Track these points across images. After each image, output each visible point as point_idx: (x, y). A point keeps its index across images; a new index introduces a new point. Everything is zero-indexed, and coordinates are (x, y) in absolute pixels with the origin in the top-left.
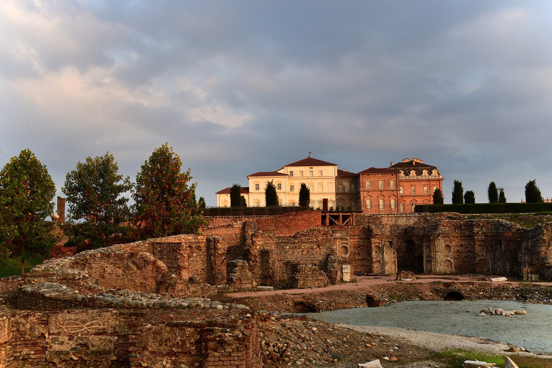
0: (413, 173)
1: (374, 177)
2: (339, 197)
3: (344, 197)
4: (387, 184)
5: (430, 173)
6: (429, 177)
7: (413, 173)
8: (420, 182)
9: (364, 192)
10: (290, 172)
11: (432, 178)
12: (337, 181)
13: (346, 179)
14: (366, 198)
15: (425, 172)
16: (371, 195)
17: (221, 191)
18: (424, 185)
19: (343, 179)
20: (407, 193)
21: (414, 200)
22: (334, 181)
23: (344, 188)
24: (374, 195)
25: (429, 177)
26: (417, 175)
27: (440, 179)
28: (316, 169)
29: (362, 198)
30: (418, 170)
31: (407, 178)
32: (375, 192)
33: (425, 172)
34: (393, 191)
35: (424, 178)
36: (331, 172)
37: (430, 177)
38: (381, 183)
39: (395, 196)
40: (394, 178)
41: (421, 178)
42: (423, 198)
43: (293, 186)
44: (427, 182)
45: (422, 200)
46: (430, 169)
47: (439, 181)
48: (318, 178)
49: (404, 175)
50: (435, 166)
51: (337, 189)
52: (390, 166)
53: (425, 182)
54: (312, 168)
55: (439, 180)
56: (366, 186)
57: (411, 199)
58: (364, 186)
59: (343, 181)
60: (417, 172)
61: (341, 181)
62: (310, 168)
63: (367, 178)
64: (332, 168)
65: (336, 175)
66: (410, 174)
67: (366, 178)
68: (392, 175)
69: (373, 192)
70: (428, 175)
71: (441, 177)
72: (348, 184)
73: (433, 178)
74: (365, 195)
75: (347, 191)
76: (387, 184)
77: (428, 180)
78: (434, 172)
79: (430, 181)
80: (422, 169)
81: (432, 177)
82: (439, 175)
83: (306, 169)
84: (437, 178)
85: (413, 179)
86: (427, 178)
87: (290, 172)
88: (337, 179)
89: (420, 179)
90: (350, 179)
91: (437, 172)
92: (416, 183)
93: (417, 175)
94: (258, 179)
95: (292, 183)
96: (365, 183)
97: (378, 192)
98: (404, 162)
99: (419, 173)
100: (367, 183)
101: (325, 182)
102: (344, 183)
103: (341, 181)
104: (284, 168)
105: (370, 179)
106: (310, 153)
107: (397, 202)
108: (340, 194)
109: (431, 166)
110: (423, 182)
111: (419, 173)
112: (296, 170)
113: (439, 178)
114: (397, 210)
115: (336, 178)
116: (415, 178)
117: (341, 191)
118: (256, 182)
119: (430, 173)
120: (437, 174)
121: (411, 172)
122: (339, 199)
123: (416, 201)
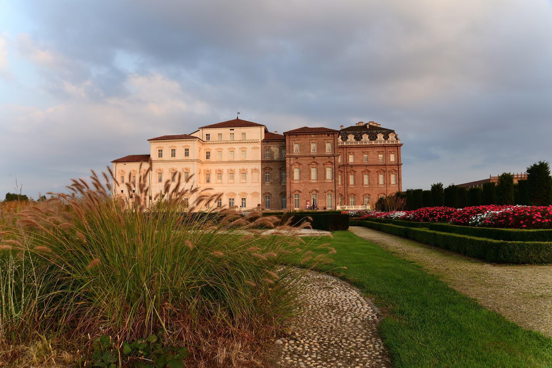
0: (365, 137)
1: (304, 139)
2: (266, 166)
3: (271, 166)
4: (321, 147)
5: (386, 137)
6: (385, 142)
7: (365, 137)
8: (373, 148)
9: (291, 158)
10: (207, 135)
11: (389, 144)
12: (263, 146)
13: (275, 143)
14: (293, 166)
15: (380, 137)
16: (300, 162)
17: (121, 159)
18: (379, 153)
19: (270, 143)
20: (358, 162)
21: (367, 170)
22: (260, 146)
23: (272, 154)
24: (305, 162)
25: (385, 142)
26: (370, 140)
27: (398, 144)
28: (238, 131)
29: (288, 166)
30: (372, 134)
31: (359, 143)
32: (305, 158)
33: (380, 137)
34: (329, 156)
35: (379, 143)
36: (257, 134)
37: (387, 143)
38: (313, 146)
39: (332, 163)
40: (331, 140)
41: (375, 144)
42: (377, 168)
43: (209, 153)
44: (382, 148)
45: (377, 170)
46: (387, 133)
47: (398, 146)
48: (240, 142)
49: (354, 140)
50: (393, 130)
51: (263, 155)
52: (341, 129)
53: (380, 148)
54: (233, 130)
55: (398, 146)
56: (293, 151)
57: (363, 170)
58: (291, 150)
59: (271, 145)
60: (370, 137)
61: (269, 146)
62: (231, 130)
63: (296, 139)
64: (258, 129)
65: (263, 138)
66: (362, 138)
67: (293, 139)
68: (328, 135)
69: (303, 158)
70: (384, 139)
71: (399, 142)
72: (278, 149)
73: (390, 143)
74: (292, 162)
75: (275, 158)
76: (321, 147)
77: (384, 146)
78: (391, 137)
79: (386, 148)
80: (377, 132)
81: (388, 142)
82: (397, 139)
83: (226, 131)
84: (395, 143)
85: (366, 145)
86: (383, 143)
87: (207, 135)
88: (264, 143)
89: (373, 145)
90: (280, 143)
91: (394, 136)
92: (369, 150)
93: (370, 140)
94: (161, 143)
95: (209, 149)
96: (293, 147)
97: (310, 158)
98: (357, 125)
99: (373, 137)
100: (296, 147)
101: (249, 147)
102: (271, 148)
103: (269, 146)
104: (199, 130)
105: (300, 141)
106: (239, 113)
107: (334, 171)
108: (267, 162)
109: (388, 130)
110: (378, 148)
111: (373, 137)
112: (214, 132)
113: (397, 143)
114: (334, 181)
115: (263, 141)
116: (368, 144)
117: (268, 158)
118: (159, 147)
119: (386, 137)
120: (395, 139)
121: (363, 136)
122: (266, 168)
123: (369, 171)
